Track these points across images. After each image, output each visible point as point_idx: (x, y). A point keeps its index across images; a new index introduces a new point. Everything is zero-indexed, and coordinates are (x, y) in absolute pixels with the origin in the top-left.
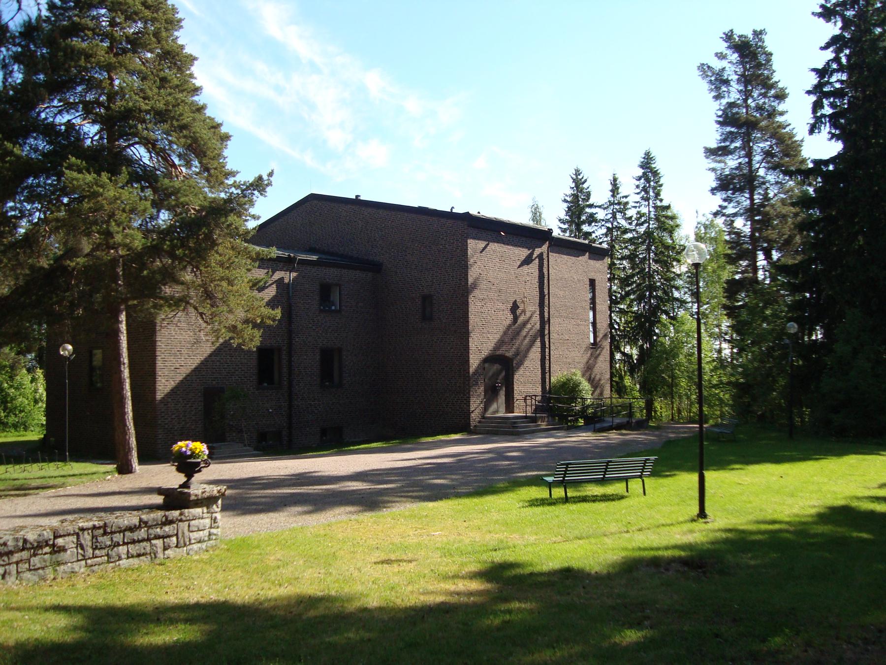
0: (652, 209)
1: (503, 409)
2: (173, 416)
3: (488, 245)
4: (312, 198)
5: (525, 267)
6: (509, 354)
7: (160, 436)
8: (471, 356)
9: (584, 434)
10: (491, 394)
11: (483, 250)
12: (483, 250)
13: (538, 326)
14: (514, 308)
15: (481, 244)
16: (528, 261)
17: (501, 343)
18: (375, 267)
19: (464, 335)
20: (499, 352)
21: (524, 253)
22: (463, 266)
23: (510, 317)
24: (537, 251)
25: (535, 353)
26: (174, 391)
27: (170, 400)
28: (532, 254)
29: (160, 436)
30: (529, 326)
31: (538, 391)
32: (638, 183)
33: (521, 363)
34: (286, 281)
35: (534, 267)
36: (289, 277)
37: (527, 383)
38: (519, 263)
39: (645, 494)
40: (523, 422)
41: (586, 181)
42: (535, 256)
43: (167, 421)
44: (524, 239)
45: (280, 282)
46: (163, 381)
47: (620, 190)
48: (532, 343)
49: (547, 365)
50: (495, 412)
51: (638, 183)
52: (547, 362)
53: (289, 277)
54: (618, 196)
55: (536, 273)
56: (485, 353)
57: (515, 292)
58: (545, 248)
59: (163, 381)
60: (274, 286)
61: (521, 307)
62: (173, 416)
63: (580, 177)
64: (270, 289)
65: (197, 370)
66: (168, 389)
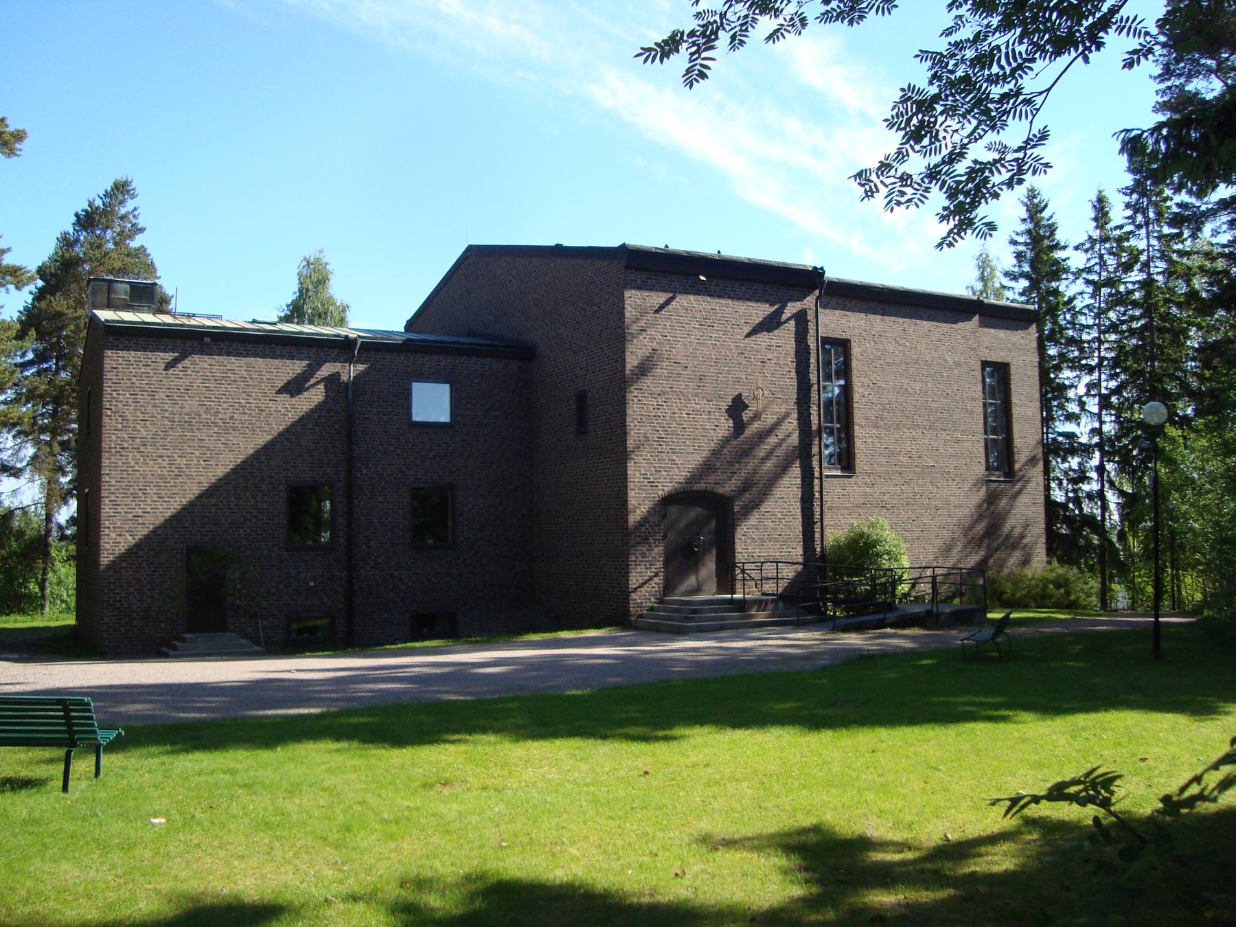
0: (1154, 242)
1: (713, 586)
2: (131, 590)
3: (673, 298)
4: (470, 249)
5: (763, 338)
6: (727, 489)
7: (106, 620)
8: (631, 494)
9: (800, 635)
10: (682, 560)
11: (662, 307)
12: (662, 307)
13: (794, 439)
14: (737, 407)
15: (659, 298)
16: (770, 324)
17: (707, 468)
18: (524, 352)
19: (616, 452)
20: (702, 486)
21: (761, 311)
22: (618, 336)
23: (726, 425)
24: (792, 308)
25: (790, 487)
26: (132, 552)
27: (124, 564)
28: (779, 312)
29: (106, 620)
30: (773, 440)
31: (798, 553)
32: (1127, 199)
33: (755, 504)
34: (344, 378)
35: (785, 337)
36: (351, 372)
37: (769, 543)
38: (747, 329)
39: (65, 788)
40: (716, 611)
41: (1046, 206)
42: (788, 313)
43: (118, 597)
44: (761, 287)
45: (332, 381)
46: (113, 535)
47: (1111, 215)
48: (783, 468)
49: (817, 509)
50: (697, 590)
51: (1127, 199)
52: (816, 504)
53: (351, 372)
54: (1108, 227)
55: (791, 346)
56: (664, 489)
57: (738, 381)
58: (810, 301)
59: (113, 535)
60: (322, 386)
61: (753, 408)
62: (131, 590)
63: (1036, 201)
64: (313, 391)
65: (176, 519)
66: (122, 548)
